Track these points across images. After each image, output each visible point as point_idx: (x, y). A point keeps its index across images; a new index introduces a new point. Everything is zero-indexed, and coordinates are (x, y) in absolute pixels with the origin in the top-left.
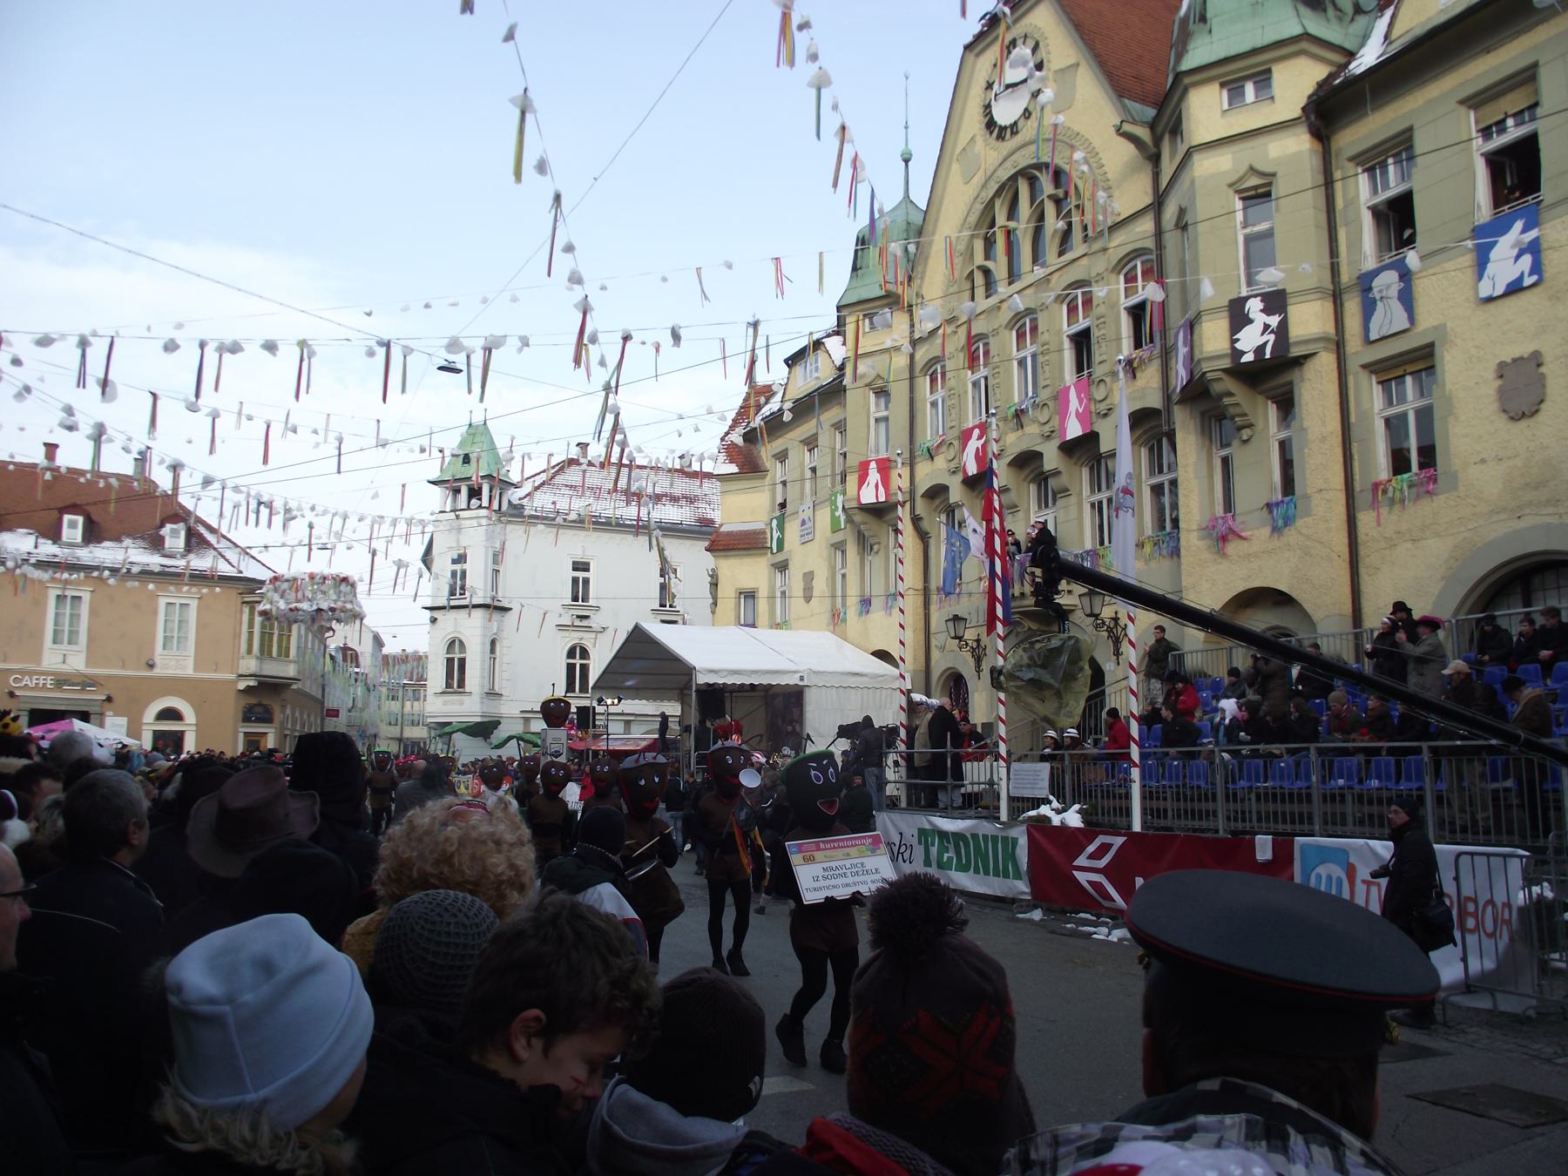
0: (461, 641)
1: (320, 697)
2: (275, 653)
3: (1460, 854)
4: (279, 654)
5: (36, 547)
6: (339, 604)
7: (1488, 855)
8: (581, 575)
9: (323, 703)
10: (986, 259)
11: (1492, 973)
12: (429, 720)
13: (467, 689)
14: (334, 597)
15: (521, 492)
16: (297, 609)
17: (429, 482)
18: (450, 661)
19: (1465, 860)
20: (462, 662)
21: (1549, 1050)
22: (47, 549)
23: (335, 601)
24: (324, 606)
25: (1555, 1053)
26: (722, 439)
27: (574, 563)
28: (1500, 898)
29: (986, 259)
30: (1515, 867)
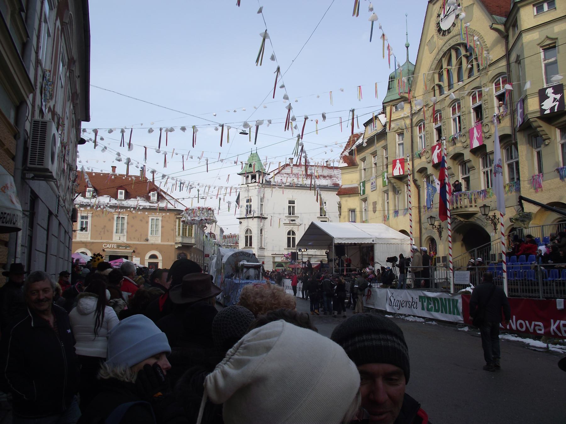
0: (250, 230)
2: (187, 236)
4: (189, 235)
5: (110, 201)
6: (208, 217)
13: (253, 247)
15: (270, 176)
16: (194, 220)
17: (238, 174)
18: (246, 237)
20: (251, 237)
22: (114, 202)
23: (207, 217)
24: (203, 218)
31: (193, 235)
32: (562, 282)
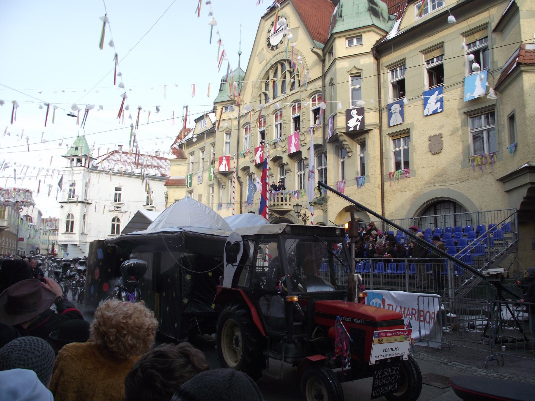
0: (72, 215)
1: (16, 233)
6: (25, 200)
8: (118, 192)
9: (17, 236)
12: (59, 243)
14: (23, 197)
15: (97, 162)
16: (8, 201)
18: (68, 222)
20: (72, 222)
23: (24, 199)
24: (19, 200)
26: (171, 147)
27: (116, 188)
31: (6, 217)
32: (412, 275)
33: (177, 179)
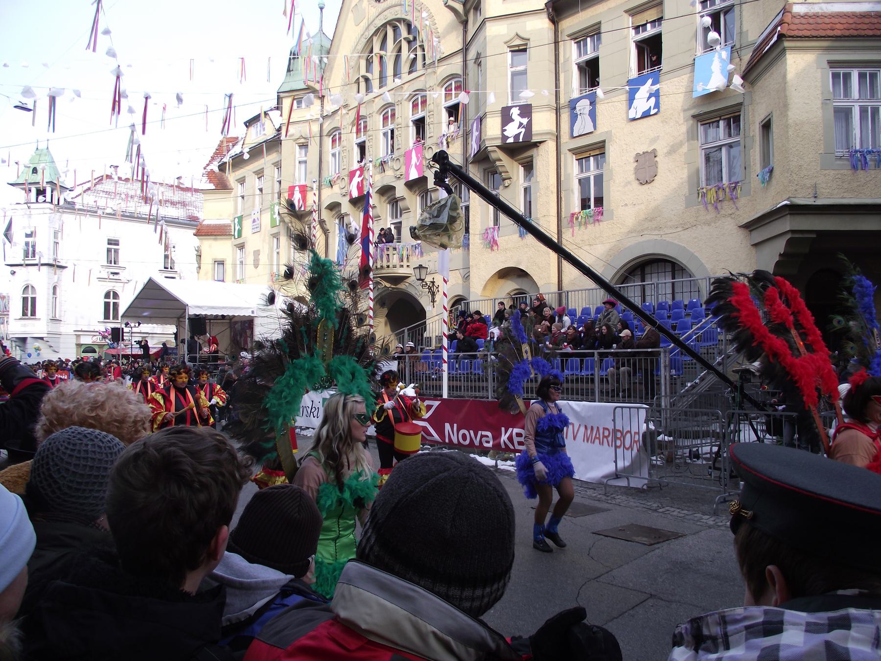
0: (32, 287)
3: (616, 408)
7: (630, 408)
10: (409, 34)
11: (629, 467)
12: (11, 336)
15: (73, 194)
18: (25, 300)
19: (618, 411)
20: (34, 300)
21: (655, 505)
25: (658, 506)
26: (205, 168)
27: (108, 240)
28: (634, 429)
29: (409, 34)
30: (643, 414)
33: (216, 225)
